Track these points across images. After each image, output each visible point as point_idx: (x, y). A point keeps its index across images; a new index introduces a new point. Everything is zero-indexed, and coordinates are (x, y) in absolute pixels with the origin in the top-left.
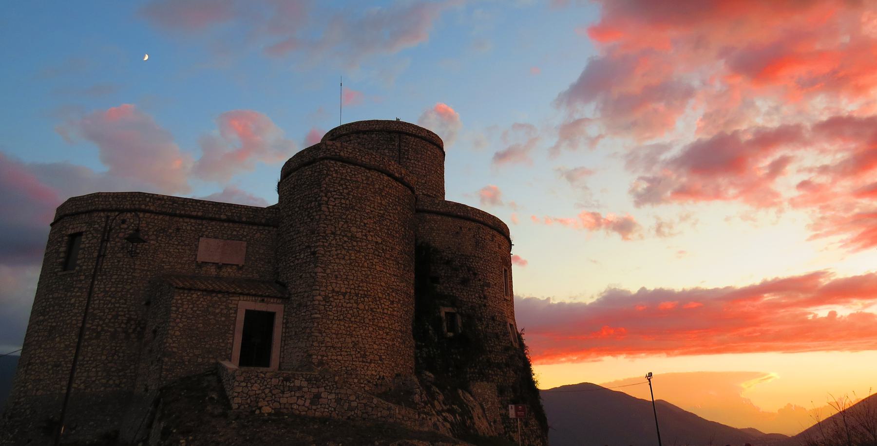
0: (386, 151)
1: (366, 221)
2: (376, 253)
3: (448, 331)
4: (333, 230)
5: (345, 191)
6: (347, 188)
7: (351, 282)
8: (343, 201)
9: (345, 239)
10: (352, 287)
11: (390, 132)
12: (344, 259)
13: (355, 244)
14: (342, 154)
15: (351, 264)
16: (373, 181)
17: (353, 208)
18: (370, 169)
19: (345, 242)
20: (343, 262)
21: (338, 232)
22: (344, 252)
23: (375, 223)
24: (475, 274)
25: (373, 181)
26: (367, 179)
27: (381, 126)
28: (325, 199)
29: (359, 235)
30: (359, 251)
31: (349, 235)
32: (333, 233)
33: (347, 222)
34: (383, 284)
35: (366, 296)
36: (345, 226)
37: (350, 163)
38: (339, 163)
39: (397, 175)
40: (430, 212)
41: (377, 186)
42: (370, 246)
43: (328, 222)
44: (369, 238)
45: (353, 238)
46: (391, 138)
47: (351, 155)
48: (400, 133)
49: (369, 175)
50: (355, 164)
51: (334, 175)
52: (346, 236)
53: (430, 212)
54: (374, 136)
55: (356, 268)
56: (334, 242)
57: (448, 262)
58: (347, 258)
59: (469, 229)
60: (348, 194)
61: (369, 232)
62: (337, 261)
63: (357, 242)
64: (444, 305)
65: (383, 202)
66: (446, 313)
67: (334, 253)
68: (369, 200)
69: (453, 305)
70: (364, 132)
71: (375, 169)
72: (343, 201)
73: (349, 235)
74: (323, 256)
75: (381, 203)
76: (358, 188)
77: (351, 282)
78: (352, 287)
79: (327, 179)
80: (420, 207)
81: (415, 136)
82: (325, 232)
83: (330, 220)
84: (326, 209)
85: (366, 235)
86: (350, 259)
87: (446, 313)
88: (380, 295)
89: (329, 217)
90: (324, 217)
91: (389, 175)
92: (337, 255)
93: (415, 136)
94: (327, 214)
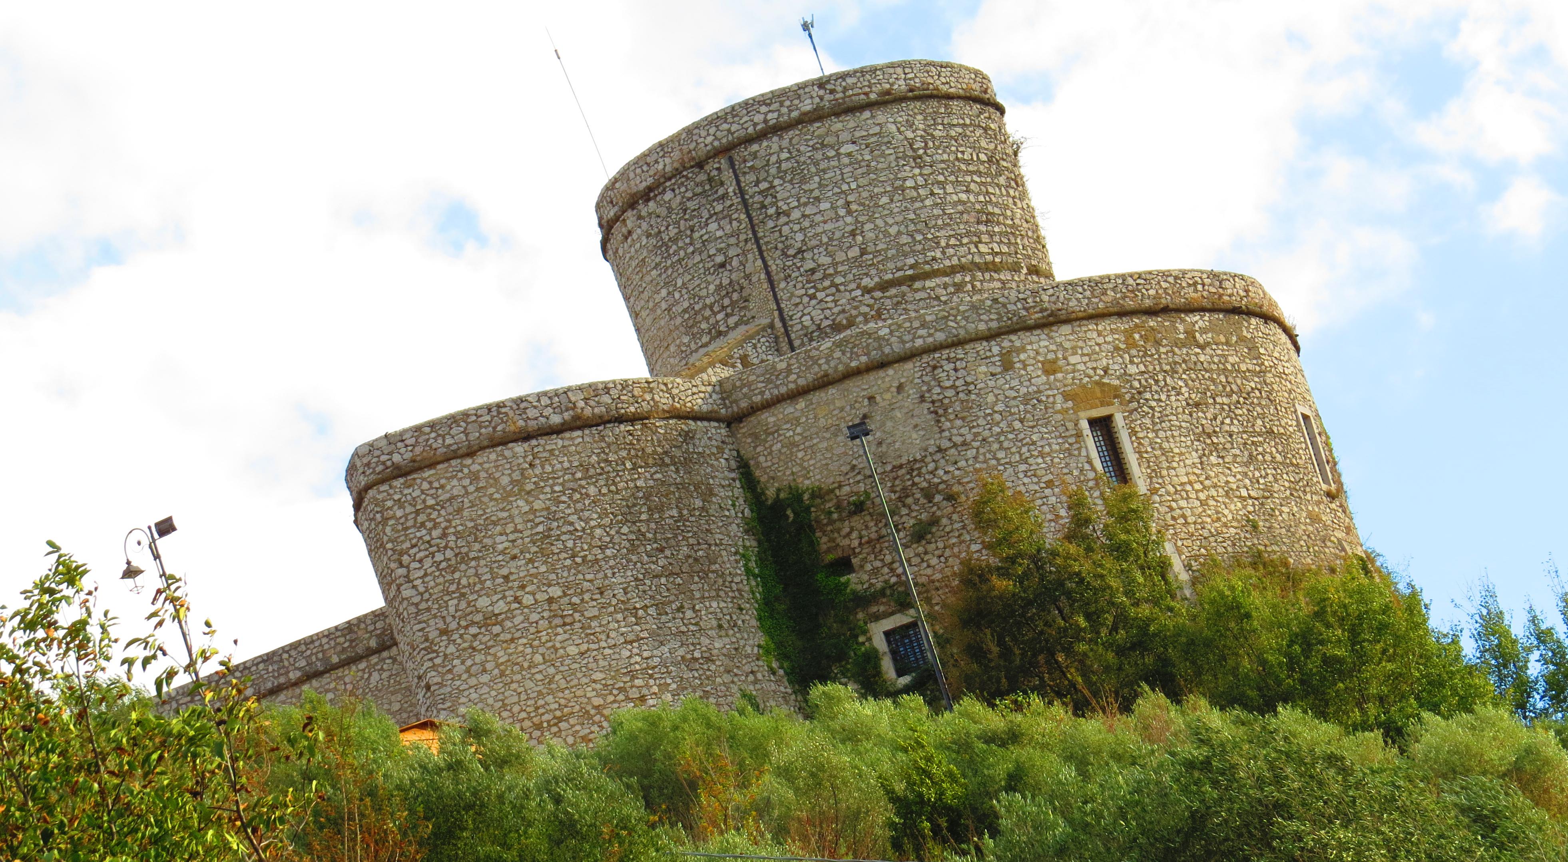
0: (713, 226)
1: (505, 571)
2: (558, 621)
3: (900, 674)
4: (441, 625)
5: (436, 533)
6: (435, 526)
7: (516, 709)
8: (439, 557)
9: (473, 630)
10: (523, 715)
11: (700, 165)
12: (484, 671)
13: (497, 629)
14: (397, 458)
15: (503, 674)
16: (490, 476)
17: (464, 558)
18: (471, 454)
19: (475, 636)
20: (485, 678)
21: (453, 626)
22: (479, 658)
23: (531, 561)
24: (950, 497)
25: (490, 476)
26: (474, 477)
27: (676, 155)
28: (402, 571)
29: (501, 607)
30: (512, 640)
31: (478, 618)
32: (444, 632)
33: (463, 595)
34: (598, 676)
35: (560, 719)
36: (463, 605)
37: (420, 469)
38: (398, 483)
39: (556, 419)
40: (767, 405)
41: (505, 480)
42: (534, 617)
43: (425, 617)
44: (528, 600)
45: (490, 619)
46: (710, 180)
47: (418, 450)
48: (726, 150)
49: (475, 467)
50: (432, 465)
51: (399, 513)
52: (473, 623)
53: (767, 405)
54: (668, 196)
55: (518, 677)
56: (452, 649)
57: (859, 508)
58: (489, 666)
59: (900, 388)
60: (444, 535)
61: (523, 587)
62: (473, 681)
63: (501, 624)
64: (877, 617)
65: (538, 505)
66: (887, 634)
67: (460, 669)
68: (495, 523)
69: (904, 604)
70: (647, 195)
71: (482, 448)
72: (439, 557)
73: (478, 618)
74: (441, 685)
75: (533, 511)
76: (459, 511)
77: (516, 709)
78: (523, 715)
79: (388, 530)
80: (744, 404)
81: (777, 129)
82: (427, 640)
83: (428, 609)
84: (414, 592)
85: (517, 600)
86: (498, 666)
87: (887, 634)
88: (597, 701)
89: (423, 605)
90: (413, 609)
91: (527, 437)
92: (468, 671)
93: (777, 129)
94: (416, 600)
